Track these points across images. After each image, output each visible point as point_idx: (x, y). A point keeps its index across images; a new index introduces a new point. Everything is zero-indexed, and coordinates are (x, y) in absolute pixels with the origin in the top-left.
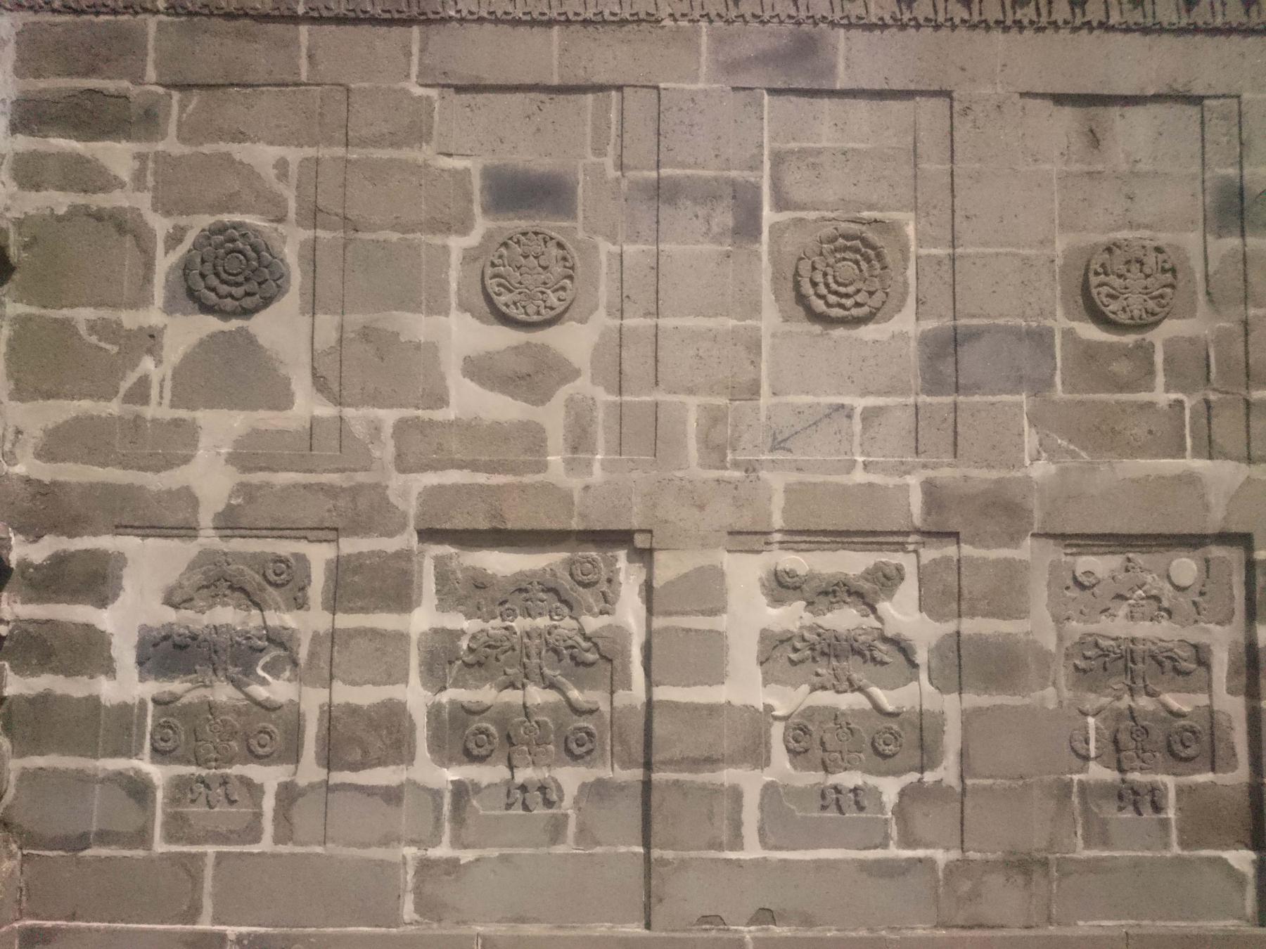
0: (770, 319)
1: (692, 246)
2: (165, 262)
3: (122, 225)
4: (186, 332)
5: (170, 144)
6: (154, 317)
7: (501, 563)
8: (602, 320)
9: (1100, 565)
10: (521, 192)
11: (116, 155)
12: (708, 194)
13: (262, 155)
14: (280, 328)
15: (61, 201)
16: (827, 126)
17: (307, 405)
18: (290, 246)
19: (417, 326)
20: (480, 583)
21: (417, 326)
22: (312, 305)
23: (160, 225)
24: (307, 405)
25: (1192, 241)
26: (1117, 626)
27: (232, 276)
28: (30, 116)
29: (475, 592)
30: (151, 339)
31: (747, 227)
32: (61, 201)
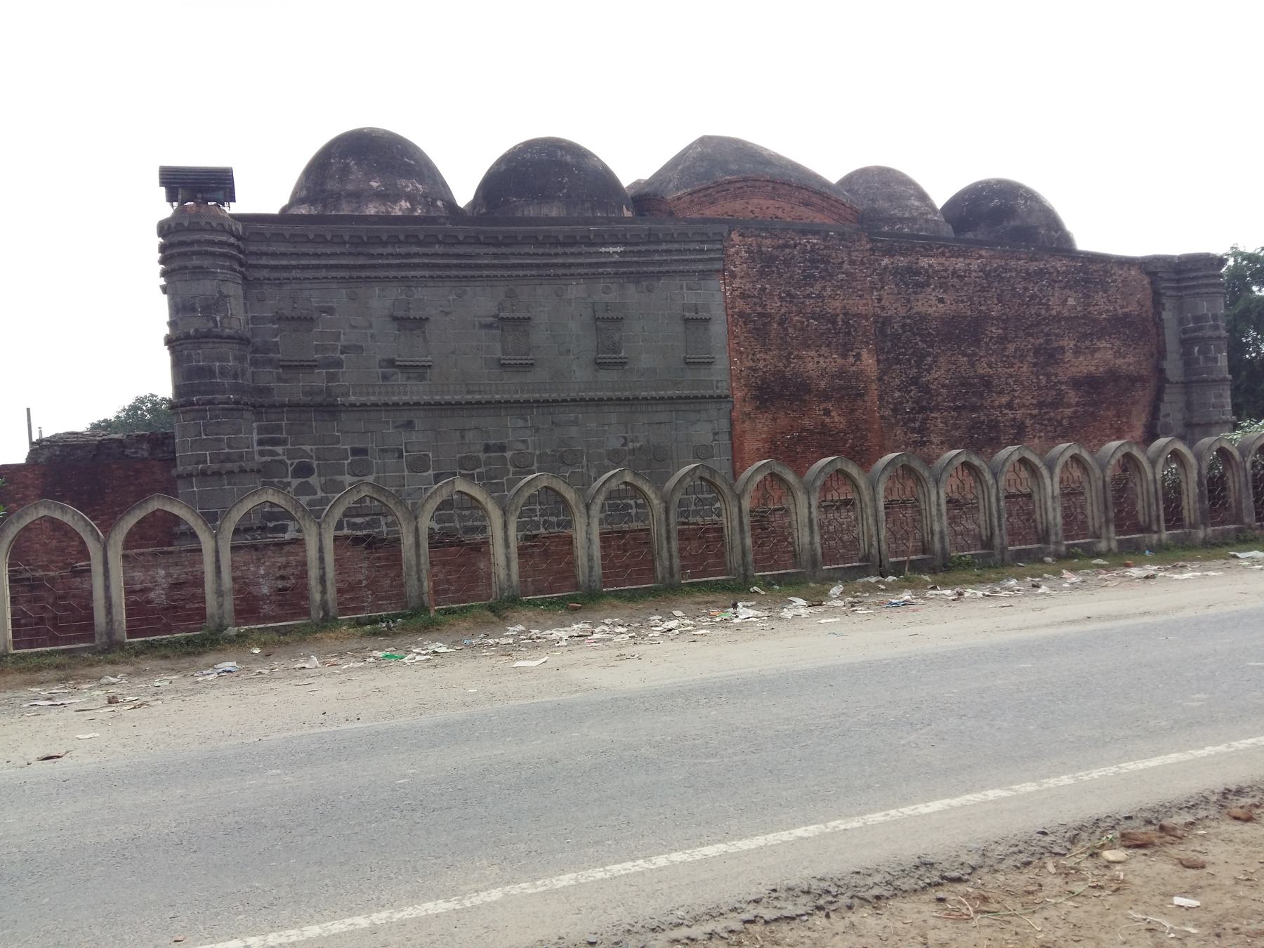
0: (406, 473)
1: (391, 461)
2: (290, 469)
3: (282, 462)
4: (295, 482)
5: (289, 447)
6: (289, 479)
7: (359, 520)
8: (374, 475)
9: (466, 513)
10: (356, 452)
11: (279, 449)
12: (392, 451)
13: (307, 448)
14: (313, 480)
15: (269, 459)
16: (414, 437)
17: (320, 494)
18: (315, 463)
19: (339, 478)
20: (355, 524)
21: (339, 478)
22: (319, 475)
23: (289, 462)
24: (320, 494)
25: (481, 455)
26: (470, 523)
27: (304, 470)
28: (260, 443)
29: (353, 526)
30: (289, 484)
31: (401, 456)
32: (269, 459)
